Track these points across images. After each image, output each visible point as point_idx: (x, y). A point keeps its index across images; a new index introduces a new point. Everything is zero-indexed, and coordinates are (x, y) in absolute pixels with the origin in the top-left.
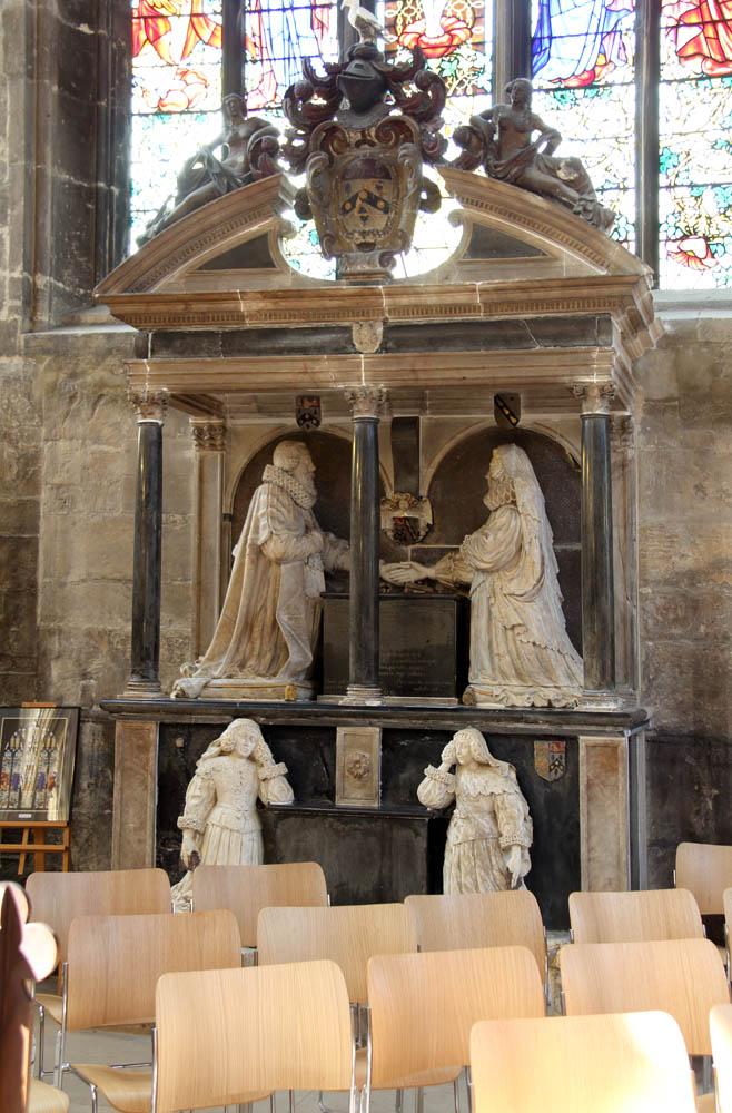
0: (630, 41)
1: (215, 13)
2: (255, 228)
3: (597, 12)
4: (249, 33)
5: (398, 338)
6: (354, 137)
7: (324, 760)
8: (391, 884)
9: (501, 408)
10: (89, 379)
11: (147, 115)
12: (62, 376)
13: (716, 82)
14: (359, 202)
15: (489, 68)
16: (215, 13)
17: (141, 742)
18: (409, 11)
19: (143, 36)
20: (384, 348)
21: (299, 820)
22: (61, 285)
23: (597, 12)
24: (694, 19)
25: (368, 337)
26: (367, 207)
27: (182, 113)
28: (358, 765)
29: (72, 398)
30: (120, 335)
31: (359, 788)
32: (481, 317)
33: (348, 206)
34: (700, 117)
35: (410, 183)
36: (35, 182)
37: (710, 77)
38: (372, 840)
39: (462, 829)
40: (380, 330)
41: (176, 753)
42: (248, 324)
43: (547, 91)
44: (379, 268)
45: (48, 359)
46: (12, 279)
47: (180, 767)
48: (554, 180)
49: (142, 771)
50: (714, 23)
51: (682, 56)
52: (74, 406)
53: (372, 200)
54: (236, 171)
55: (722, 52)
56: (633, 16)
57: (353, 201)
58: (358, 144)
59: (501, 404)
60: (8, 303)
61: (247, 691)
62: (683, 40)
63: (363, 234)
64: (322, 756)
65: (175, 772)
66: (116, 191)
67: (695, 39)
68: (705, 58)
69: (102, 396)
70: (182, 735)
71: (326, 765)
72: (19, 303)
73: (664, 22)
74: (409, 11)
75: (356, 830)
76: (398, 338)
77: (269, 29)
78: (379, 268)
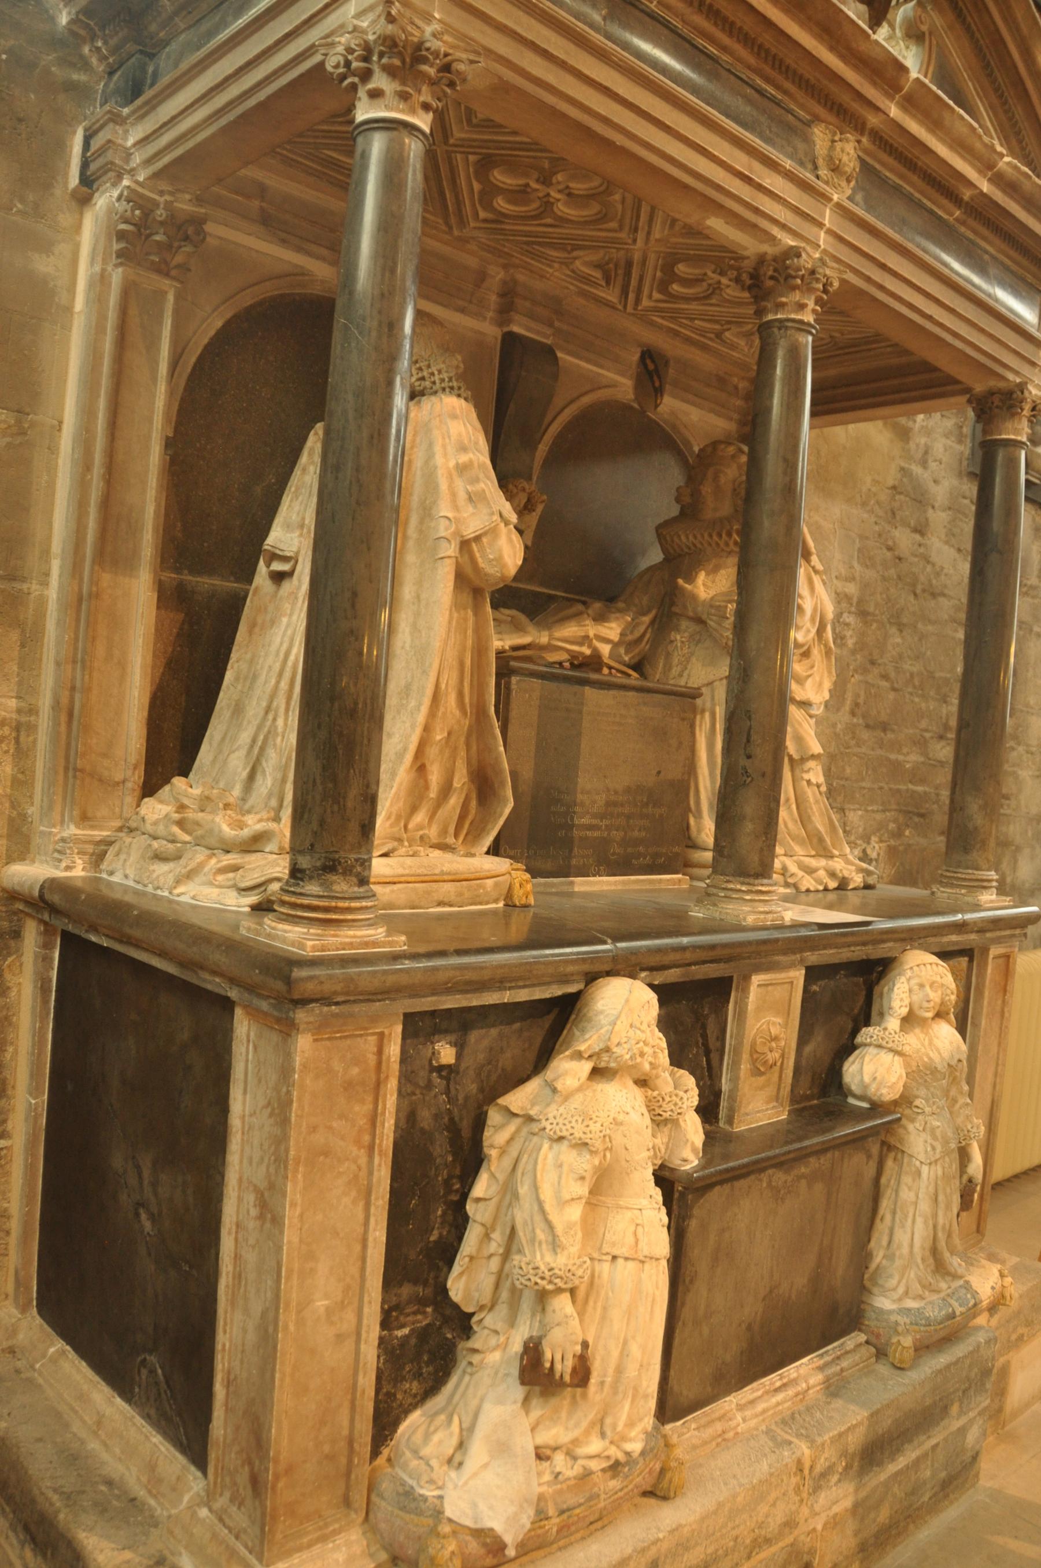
7: (706, 1045)
8: (830, 1259)
9: (650, 374)
17: (355, 1071)
21: (727, 1187)
28: (774, 1044)
31: (761, 1088)
38: (819, 1187)
39: (938, 1133)
41: (429, 1085)
47: (436, 1117)
49: (355, 1151)
59: (651, 367)
61: (448, 889)
64: (704, 1036)
65: (423, 1131)
70: (446, 1031)
71: (707, 1053)
75: (800, 1177)
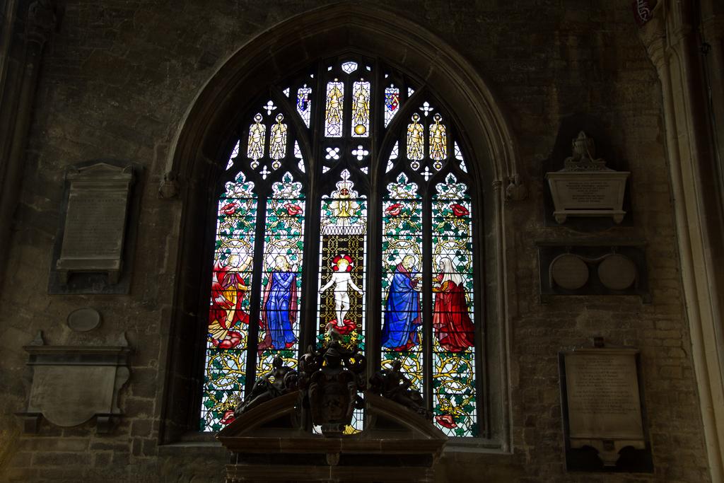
0: (421, 336)
1: (246, 310)
2: (285, 411)
3: (408, 324)
4: (261, 319)
5: (346, 460)
6: (330, 378)
10: (188, 467)
11: (213, 349)
12: (176, 465)
13: (454, 355)
14: (330, 404)
15: (364, 341)
16: (246, 310)
18: (330, 316)
19: (214, 317)
20: (340, 464)
22: (173, 423)
23: (408, 324)
24: (445, 330)
25: (332, 460)
26: (334, 406)
27: (228, 349)
29: (180, 476)
30: (204, 448)
32: (380, 452)
33: (326, 405)
34: (449, 367)
35: (352, 397)
36: (168, 379)
37: (452, 353)
40: (338, 456)
42: (281, 451)
43: (387, 352)
44: (338, 431)
45: (169, 458)
46: (155, 421)
48: (409, 400)
50: (453, 332)
51: (442, 343)
52: (181, 479)
53: (336, 403)
54: (278, 388)
55: (456, 343)
56: (421, 327)
57: (328, 403)
58: (330, 380)
60: (153, 431)
62: (441, 338)
63: (332, 416)
66: (198, 381)
67: (445, 338)
68: (450, 345)
69: (194, 475)
72: (157, 432)
73: (434, 330)
74: (330, 316)
76: (346, 460)
77: (270, 318)
78: (338, 431)
